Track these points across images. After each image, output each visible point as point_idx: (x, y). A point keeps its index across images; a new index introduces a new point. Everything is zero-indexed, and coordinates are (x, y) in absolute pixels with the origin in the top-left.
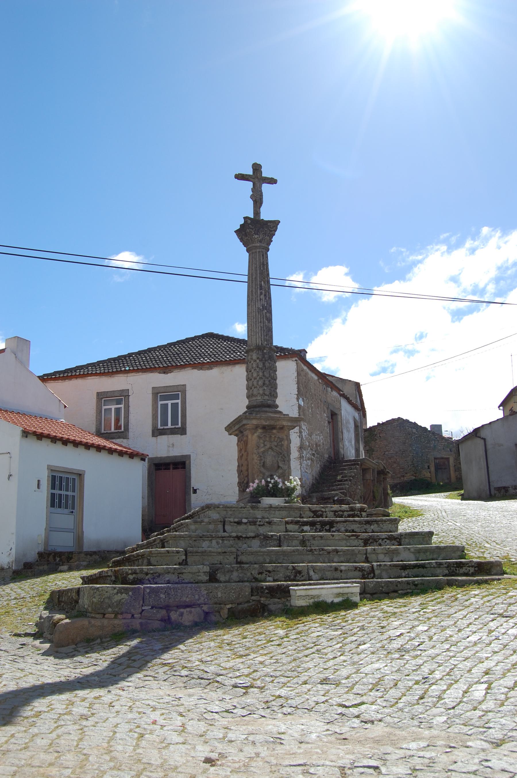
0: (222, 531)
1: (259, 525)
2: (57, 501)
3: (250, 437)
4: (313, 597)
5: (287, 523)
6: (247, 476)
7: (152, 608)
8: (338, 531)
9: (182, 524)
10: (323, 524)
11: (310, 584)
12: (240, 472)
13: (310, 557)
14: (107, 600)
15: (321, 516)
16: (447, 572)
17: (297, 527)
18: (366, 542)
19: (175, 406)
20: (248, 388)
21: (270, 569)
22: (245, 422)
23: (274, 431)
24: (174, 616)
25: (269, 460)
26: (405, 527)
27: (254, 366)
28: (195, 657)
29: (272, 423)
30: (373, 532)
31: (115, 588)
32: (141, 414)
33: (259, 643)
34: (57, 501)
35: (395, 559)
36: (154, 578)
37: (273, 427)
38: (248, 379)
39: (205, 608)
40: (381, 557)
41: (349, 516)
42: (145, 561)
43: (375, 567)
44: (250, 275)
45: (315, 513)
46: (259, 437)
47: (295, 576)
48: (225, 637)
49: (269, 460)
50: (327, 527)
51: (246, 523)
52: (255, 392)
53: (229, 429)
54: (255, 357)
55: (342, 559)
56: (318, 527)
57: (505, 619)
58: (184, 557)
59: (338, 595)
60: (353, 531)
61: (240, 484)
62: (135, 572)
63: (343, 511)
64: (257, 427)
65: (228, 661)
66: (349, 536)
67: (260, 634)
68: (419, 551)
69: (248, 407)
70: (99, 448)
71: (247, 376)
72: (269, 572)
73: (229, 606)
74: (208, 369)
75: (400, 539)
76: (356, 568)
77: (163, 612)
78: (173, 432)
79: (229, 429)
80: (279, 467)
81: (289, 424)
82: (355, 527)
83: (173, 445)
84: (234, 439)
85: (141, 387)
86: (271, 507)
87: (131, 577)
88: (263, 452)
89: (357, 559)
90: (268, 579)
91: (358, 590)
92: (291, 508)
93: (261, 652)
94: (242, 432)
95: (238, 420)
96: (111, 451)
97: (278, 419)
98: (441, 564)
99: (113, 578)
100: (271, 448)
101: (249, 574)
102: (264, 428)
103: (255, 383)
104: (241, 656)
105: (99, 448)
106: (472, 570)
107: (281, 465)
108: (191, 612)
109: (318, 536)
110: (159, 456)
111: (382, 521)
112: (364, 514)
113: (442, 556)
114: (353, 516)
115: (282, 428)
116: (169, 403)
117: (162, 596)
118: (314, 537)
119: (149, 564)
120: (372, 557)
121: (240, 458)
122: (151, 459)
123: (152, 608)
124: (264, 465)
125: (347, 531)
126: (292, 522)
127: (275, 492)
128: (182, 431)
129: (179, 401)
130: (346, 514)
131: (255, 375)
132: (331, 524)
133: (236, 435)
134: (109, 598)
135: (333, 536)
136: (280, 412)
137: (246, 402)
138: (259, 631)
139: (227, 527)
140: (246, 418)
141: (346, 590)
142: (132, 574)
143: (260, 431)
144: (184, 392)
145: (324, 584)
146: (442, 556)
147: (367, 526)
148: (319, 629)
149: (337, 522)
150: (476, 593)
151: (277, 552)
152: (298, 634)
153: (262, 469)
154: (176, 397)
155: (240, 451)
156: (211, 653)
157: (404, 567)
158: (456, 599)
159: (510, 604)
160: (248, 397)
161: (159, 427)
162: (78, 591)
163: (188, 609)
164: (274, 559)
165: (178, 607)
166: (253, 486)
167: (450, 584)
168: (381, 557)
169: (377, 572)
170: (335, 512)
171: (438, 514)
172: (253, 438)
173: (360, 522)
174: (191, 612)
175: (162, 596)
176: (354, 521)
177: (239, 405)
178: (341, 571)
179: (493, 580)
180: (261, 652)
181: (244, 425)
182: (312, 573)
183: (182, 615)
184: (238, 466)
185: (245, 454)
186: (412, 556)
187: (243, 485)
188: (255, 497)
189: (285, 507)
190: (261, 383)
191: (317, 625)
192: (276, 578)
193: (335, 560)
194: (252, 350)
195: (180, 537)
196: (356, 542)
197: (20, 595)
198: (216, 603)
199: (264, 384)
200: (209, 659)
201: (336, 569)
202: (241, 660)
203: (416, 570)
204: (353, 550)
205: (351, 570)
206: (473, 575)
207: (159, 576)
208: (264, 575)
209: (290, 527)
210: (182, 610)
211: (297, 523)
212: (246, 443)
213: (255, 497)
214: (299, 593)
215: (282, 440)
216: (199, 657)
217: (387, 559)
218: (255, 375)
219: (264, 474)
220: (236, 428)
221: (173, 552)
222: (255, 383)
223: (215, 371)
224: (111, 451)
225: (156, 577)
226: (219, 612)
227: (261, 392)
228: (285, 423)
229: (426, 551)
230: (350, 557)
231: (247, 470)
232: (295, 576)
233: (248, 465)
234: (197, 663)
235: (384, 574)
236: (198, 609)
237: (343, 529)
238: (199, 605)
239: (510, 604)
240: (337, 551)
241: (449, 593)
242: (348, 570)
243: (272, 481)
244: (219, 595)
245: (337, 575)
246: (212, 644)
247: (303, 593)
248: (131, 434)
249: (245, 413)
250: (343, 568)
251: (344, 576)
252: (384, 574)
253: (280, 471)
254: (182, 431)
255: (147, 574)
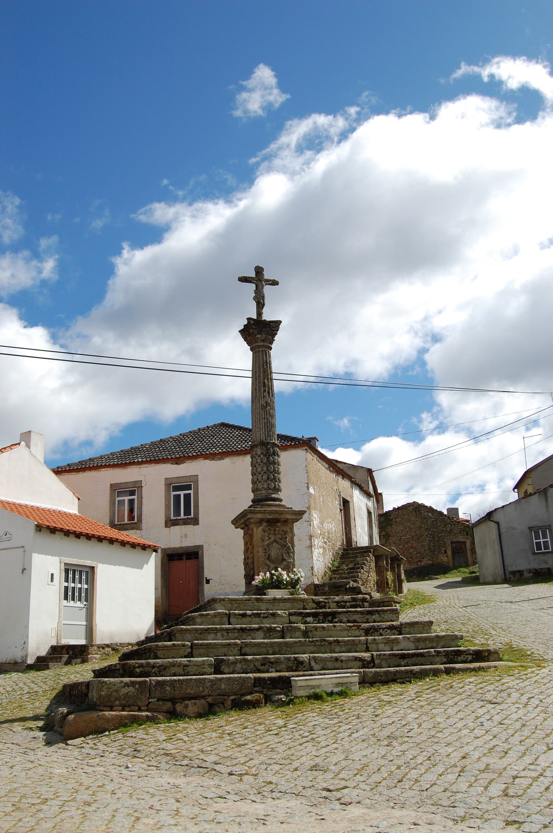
0: (227, 623)
1: (263, 617)
2: (70, 593)
3: (255, 530)
4: (313, 687)
5: (290, 614)
6: (253, 569)
7: (158, 700)
8: (341, 622)
9: (188, 617)
10: (326, 615)
11: (311, 675)
12: (246, 564)
13: (312, 648)
14: (114, 694)
15: (324, 607)
16: (445, 660)
17: (300, 618)
18: (367, 632)
19: (187, 497)
20: (254, 482)
21: (272, 660)
22: (250, 516)
23: (279, 524)
24: (179, 708)
25: (274, 552)
26: (406, 616)
27: (259, 461)
28: (196, 747)
29: (276, 516)
30: (374, 622)
31: (122, 682)
32: (154, 505)
33: (258, 733)
34: (70, 593)
35: (395, 648)
36: (160, 671)
37: (277, 521)
38: (253, 474)
39: (210, 700)
40: (381, 646)
41: (351, 607)
42: (152, 655)
43: (375, 657)
44: (254, 371)
45: (319, 604)
46: (264, 531)
47: (297, 667)
48: (226, 728)
49: (274, 552)
50: (330, 618)
51: (250, 616)
52: (260, 486)
53: (236, 522)
54: (259, 452)
55: (343, 649)
56: (321, 618)
57: (493, 706)
58: (189, 650)
59: (338, 685)
60: (355, 621)
61: (246, 576)
62: (141, 666)
63: (346, 602)
64: (261, 521)
65: (227, 751)
66: (350, 627)
67: (260, 724)
68: (418, 640)
69: (253, 501)
70: (112, 541)
71: (252, 470)
72: (272, 663)
73: (232, 698)
74: (220, 459)
75: (401, 629)
76: (356, 658)
77: (169, 705)
78: (185, 522)
79: (236, 522)
80: (283, 559)
81: (293, 517)
82: (356, 617)
83: (186, 535)
84: (241, 532)
85: (154, 479)
86: (275, 599)
87: (138, 670)
88: (268, 545)
89: (358, 649)
90: (271, 670)
91: (356, 680)
92: (294, 600)
93: (259, 741)
94: (248, 526)
95: (243, 514)
96: (123, 544)
97: (282, 513)
98: (439, 652)
99: (121, 671)
100: (275, 541)
101: (252, 666)
102: (268, 521)
103: (260, 478)
104: (240, 746)
105: (112, 541)
106: (470, 658)
107: (285, 557)
108: (195, 704)
109: (320, 627)
110: (172, 547)
111: (383, 611)
112: (366, 604)
113: (441, 644)
114: (355, 606)
115: (286, 521)
116: (182, 493)
117: (168, 688)
118: (316, 628)
119: (156, 657)
120: (372, 646)
121: (246, 551)
122: (164, 550)
123: (158, 700)
124: (269, 558)
125: (349, 621)
126: (295, 614)
127: (277, 584)
128: (195, 521)
129: (191, 492)
130: (348, 604)
131: (259, 470)
132: (334, 615)
133: (242, 528)
134: (116, 691)
135: (334, 626)
136: (283, 506)
137: (251, 496)
138: (259, 721)
139: (232, 620)
140: (251, 512)
141: (345, 680)
142: (139, 667)
143: (265, 524)
144: (196, 482)
145: (325, 674)
146: (441, 644)
147: (369, 617)
148: (316, 718)
149: (340, 613)
150: (471, 680)
151: (280, 643)
152: (296, 724)
153: (268, 562)
154: (188, 487)
155: (246, 544)
156: (211, 744)
157: (403, 657)
158: (451, 687)
159: (502, 691)
160: (253, 491)
161: (172, 518)
162: (88, 685)
163: (193, 701)
164: (277, 650)
165: (184, 699)
166: (258, 579)
167: (448, 672)
168: (381, 646)
169: (377, 662)
170: (338, 602)
171: (438, 604)
172: (258, 532)
173: (361, 613)
174: (195, 704)
175: (168, 688)
176: (356, 611)
177: (245, 499)
178: (342, 661)
179: (490, 667)
180: (259, 741)
181: (249, 519)
182: (313, 663)
183: (186, 706)
184: (245, 559)
185: (250, 547)
186: (412, 645)
187: (249, 577)
188: (261, 590)
189: (289, 599)
190: (265, 477)
191: (315, 714)
192: (278, 669)
193: (337, 650)
194: (256, 446)
195: (187, 630)
196: (357, 633)
197: (32, 689)
198: (220, 695)
199: (268, 478)
200: (209, 749)
201: (337, 659)
202: (239, 749)
203: (414, 659)
204: (354, 641)
205: (352, 660)
206: (471, 662)
207: (165, 669)
208: (267, 666)
209: (293, 618)
210: (187, 702)
211: (300, 614)
212: (251, 536)
213: (261, 590)
214: (299, 684)
215: (286, 532)
216: (200, 747)
217: (387, 648)
218: (259, 470)
219: (269, 566)
220: (242, 521)
221: (179, 645)
222: (260, 478)
223: (227, 462)
224: (123, 544)
225: (162, 670)
226: (223, 704)
227: (265, 486)
228: (289, 517)
229: (425, 639)
230: (352, 646)
231: (253, 563)
232: (297, 667)
233: (253, 558)
234: (199, 753)
235: (384, 663)
236: (203, 701)
237: (345, 620)
238: (203, 697)
239: (502, 691)
240: (338, 642)
241: (445, 680)
242: (349, 660)
243: (276, 573)
244: (223, 686)
245: (338, 664)
246: (214, 735)
247: (303, 684)
248: (144, 525)
249: (250, 507)
250: (343, 658)
251: (344, 665)
252: (384, 663)
253: (285, 563)
254: (195, 521)
255: (153, 667)
